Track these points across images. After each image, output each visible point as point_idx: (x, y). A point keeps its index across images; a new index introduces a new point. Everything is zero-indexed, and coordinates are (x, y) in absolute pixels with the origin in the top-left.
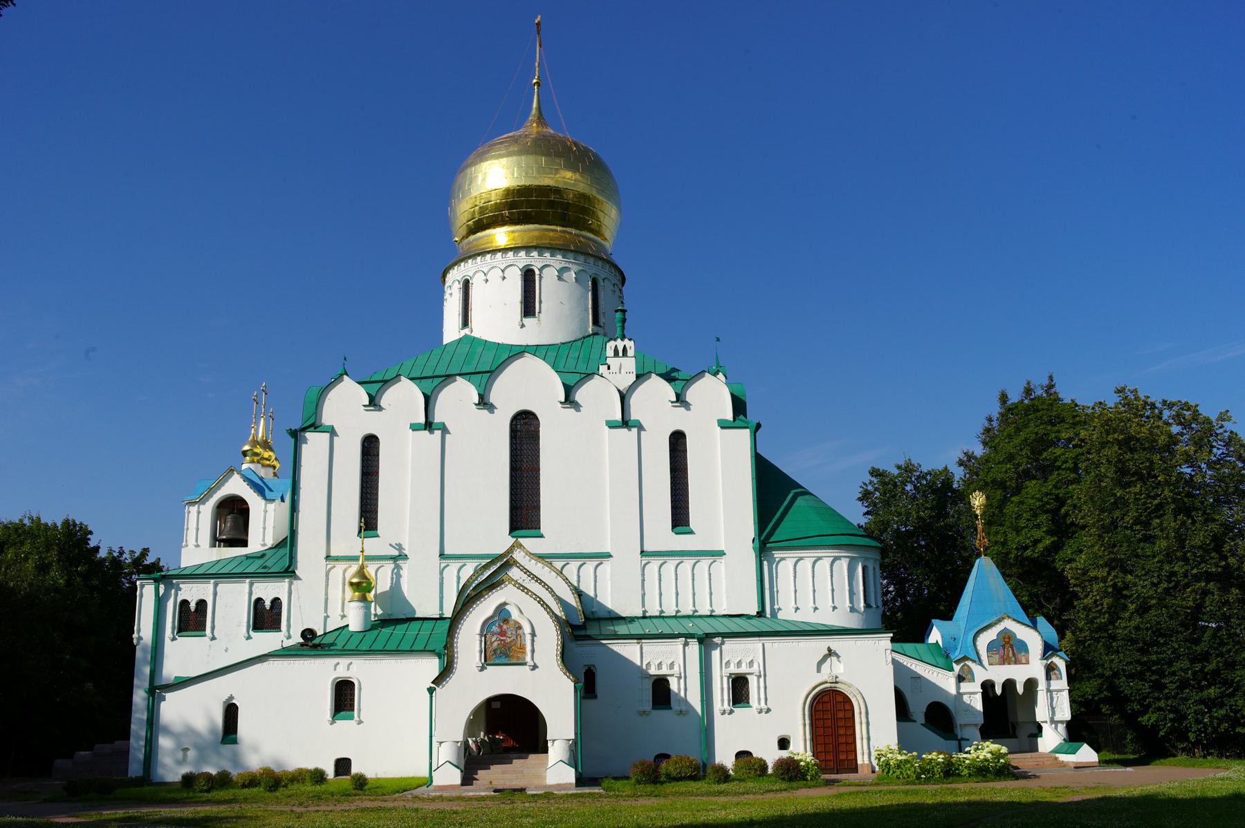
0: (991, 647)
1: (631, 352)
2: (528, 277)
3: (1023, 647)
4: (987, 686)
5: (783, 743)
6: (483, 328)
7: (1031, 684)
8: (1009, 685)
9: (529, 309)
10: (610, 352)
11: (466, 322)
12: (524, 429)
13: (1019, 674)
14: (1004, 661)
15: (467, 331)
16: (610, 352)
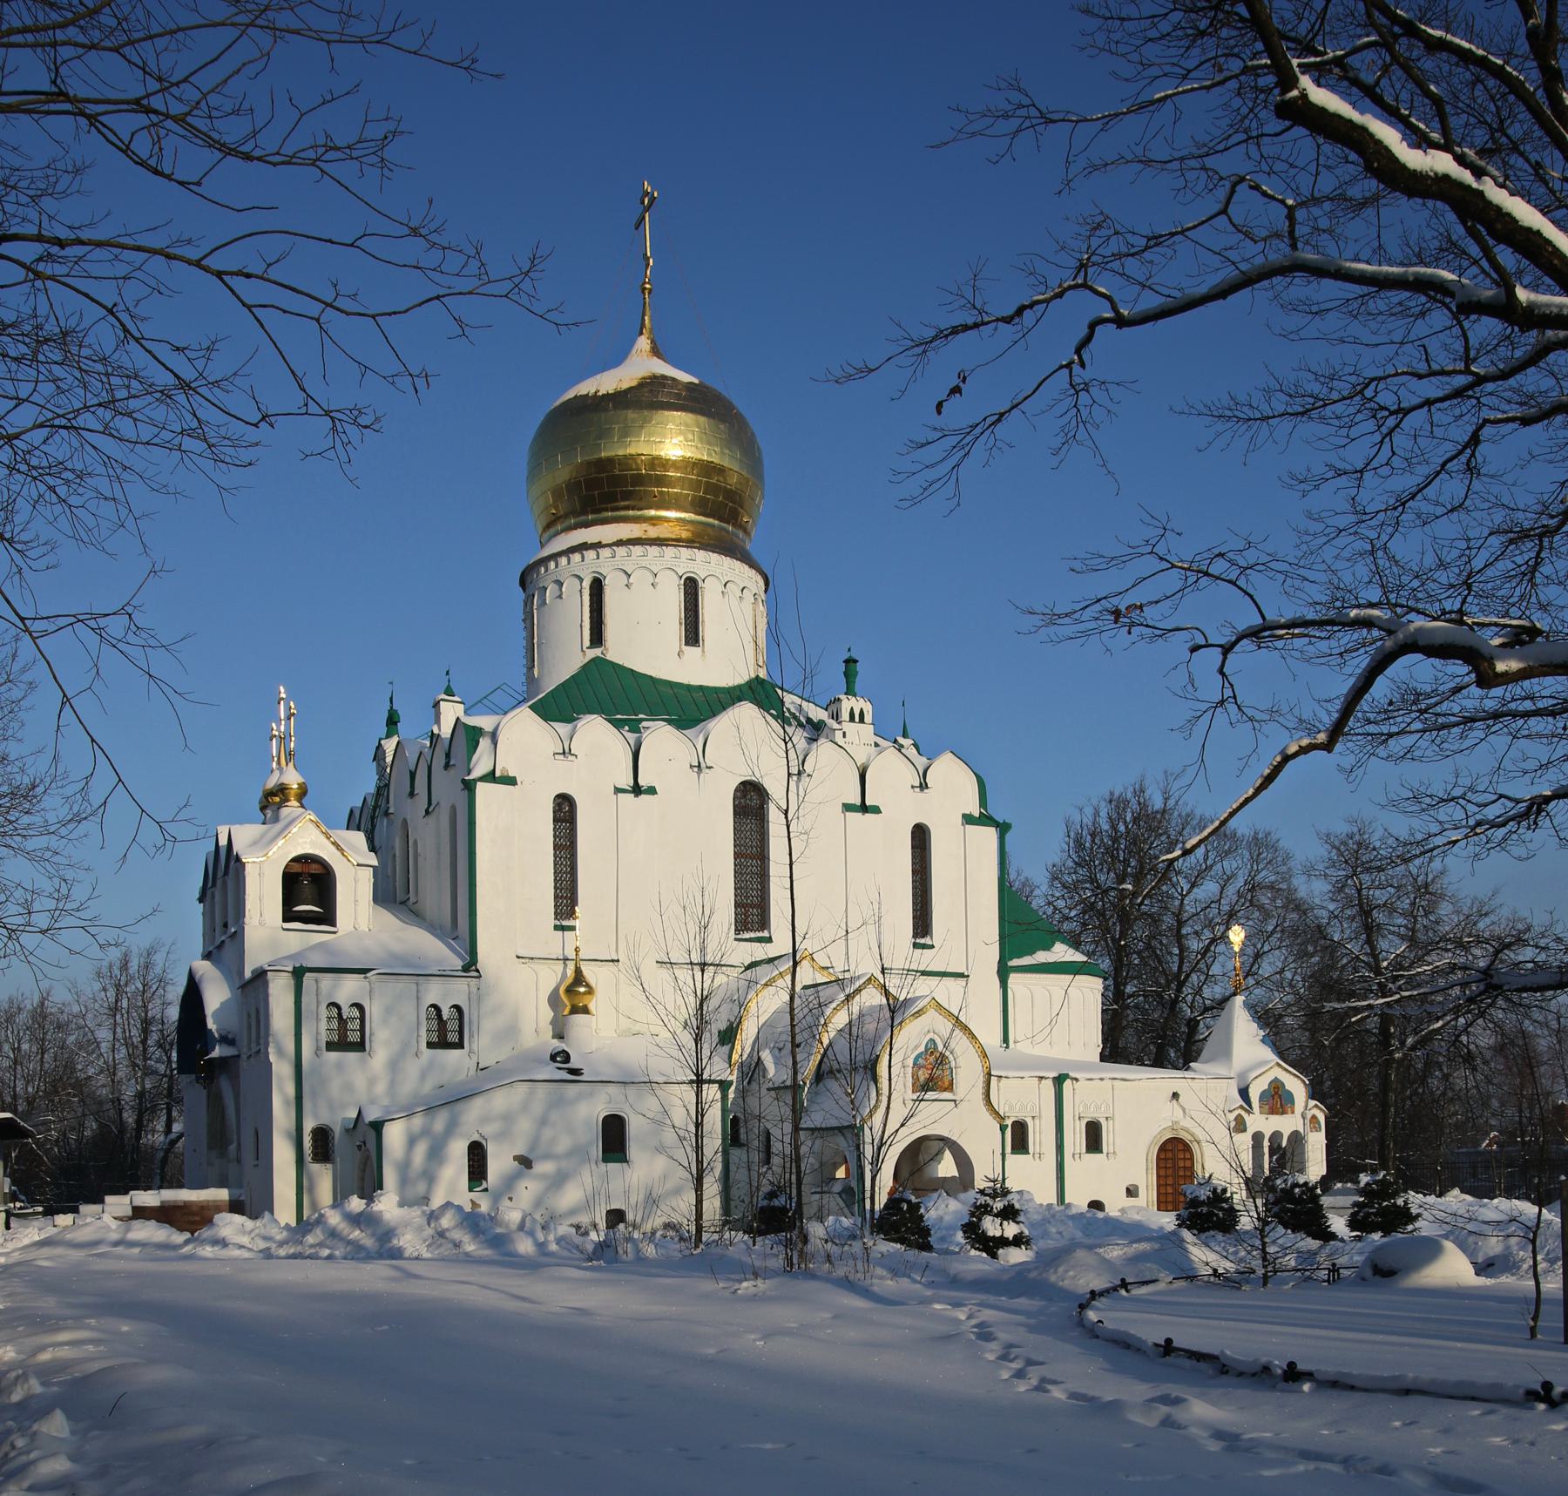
0: (1263, 1096)
1: (868, 718)
2: (691, 588)
3: (1289, 1098)
4: (1258, 1137)
5: (1131, 1192)
6: (623, 649)
7: (1297, 1138)
8: (1276, 1136)
9: (692, 635)
10: (845, 716)
11: (597, 638)
12: (751, 803)
13: (1286, 1124)
14: (1273, 1111)
15: (597, 652)
16: (845, 716)
